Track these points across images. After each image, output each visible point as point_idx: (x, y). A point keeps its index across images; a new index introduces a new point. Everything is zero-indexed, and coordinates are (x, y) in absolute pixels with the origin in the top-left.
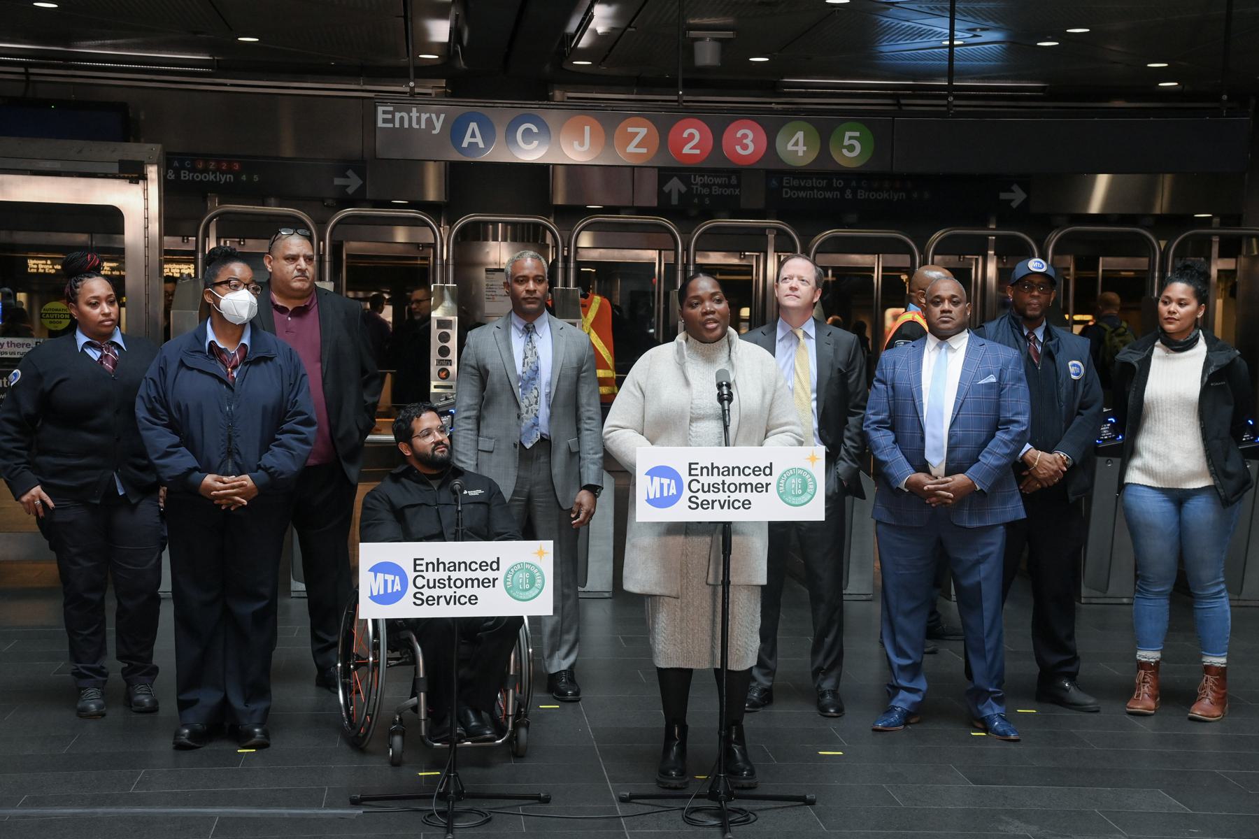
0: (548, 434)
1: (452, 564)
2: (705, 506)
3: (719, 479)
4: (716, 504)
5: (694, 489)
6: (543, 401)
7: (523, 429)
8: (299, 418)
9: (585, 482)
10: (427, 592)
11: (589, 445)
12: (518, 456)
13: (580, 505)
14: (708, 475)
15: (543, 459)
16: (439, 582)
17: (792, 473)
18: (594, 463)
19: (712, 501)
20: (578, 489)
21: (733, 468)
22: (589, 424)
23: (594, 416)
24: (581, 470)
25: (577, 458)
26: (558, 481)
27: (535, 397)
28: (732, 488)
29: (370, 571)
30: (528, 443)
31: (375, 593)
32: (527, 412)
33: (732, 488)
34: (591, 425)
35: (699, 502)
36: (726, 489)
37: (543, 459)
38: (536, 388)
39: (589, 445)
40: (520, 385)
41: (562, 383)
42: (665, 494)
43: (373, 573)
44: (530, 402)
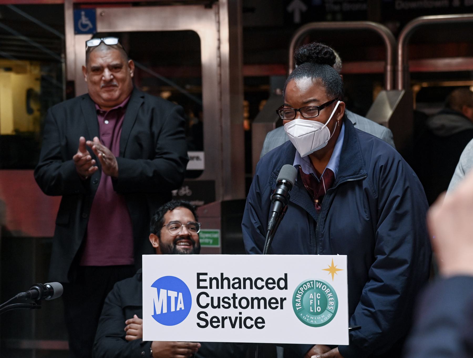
3: (229, 293)
4: (227, 322)
14: (218, 287)
17: (309, 286)
21: (245, 280)
28: (244, 303)
33: (244, 303)
35: (208, 319)
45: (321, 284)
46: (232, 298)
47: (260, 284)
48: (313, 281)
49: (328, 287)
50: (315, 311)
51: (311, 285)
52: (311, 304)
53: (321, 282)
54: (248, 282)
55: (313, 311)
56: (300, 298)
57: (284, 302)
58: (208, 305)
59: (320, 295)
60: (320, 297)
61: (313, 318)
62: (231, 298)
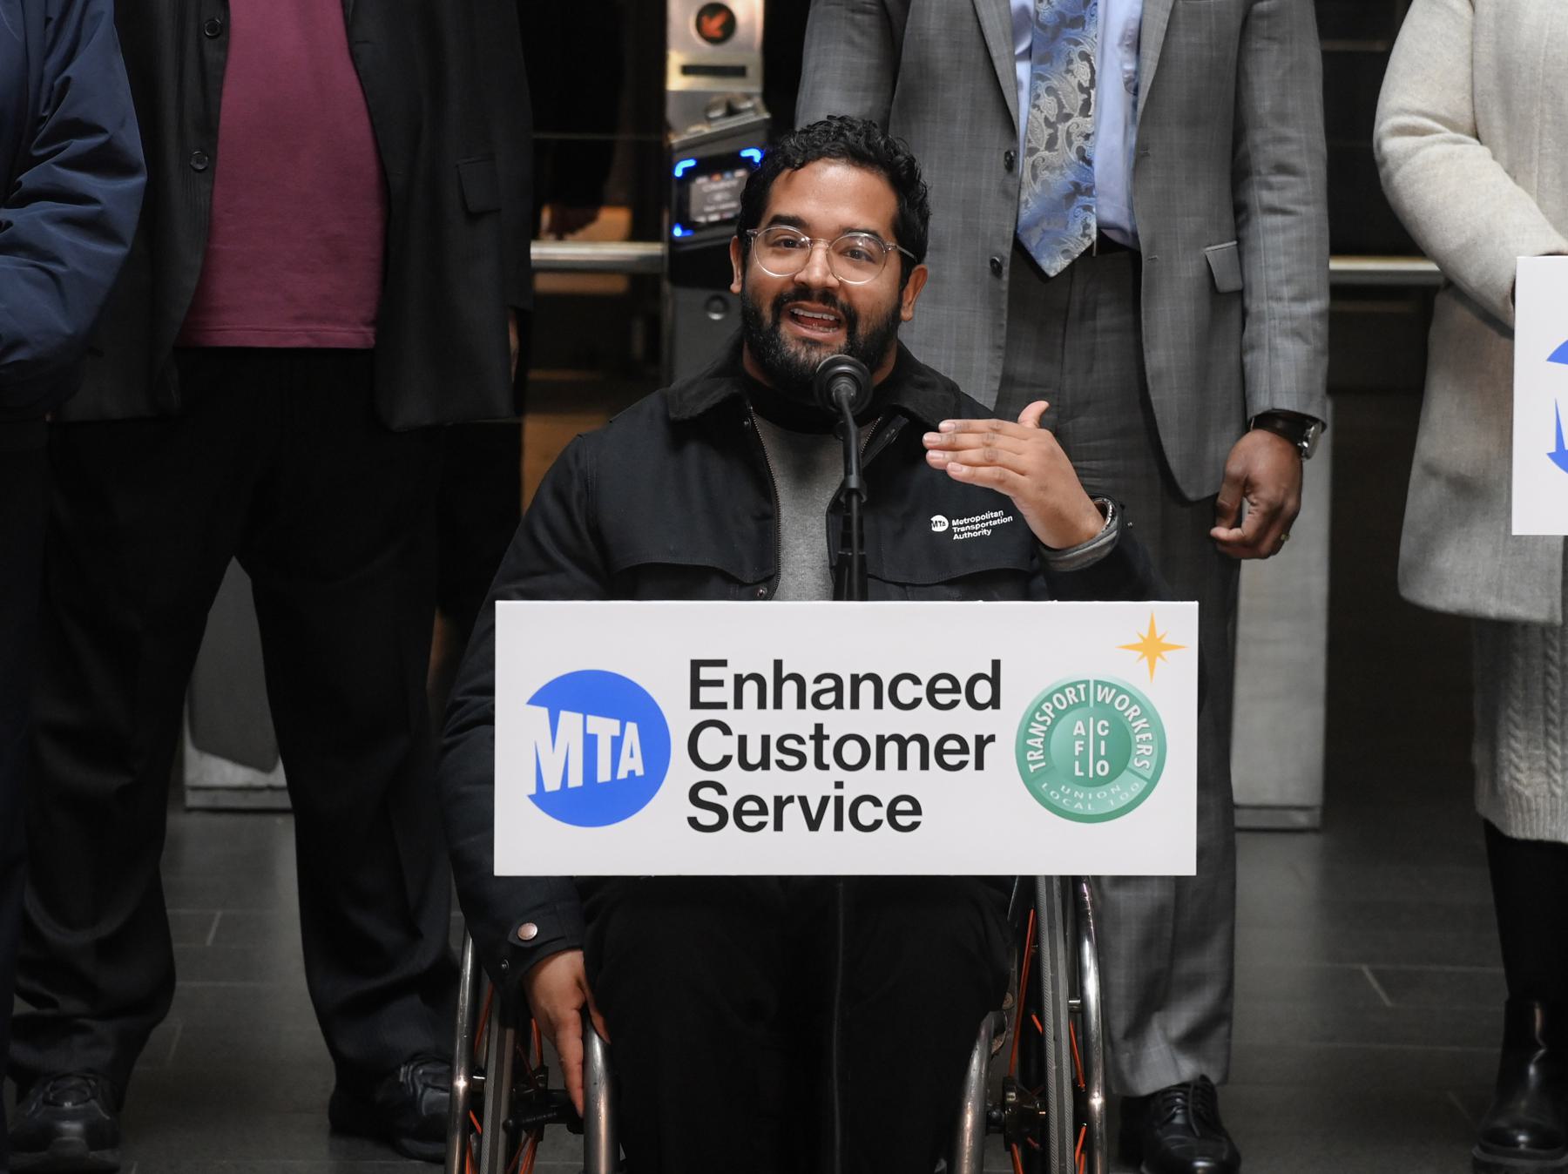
0: (1127, 226)
1: (829, 683)
2: (750, 821)
3: (802, 722)
4: (793, 813)
5: (710, 757)
6: (1112, 103)
7: (1025, 214)
8: (79, 145)
9: (1262, 403)
10: (738, 783)
11: (1277, 267)
12: (1005, 306)
13: (1246, 485)
14: (762, 704)
15: (1106, 317)
16: (781, 747)
17: (1072, 697)
18: (1297, 334)
19: (778, 800)
20: (1234, 427)
21: (856, 680)
22: (1282, 188)
23: (1296, 161)
24: (1248, 359)
25: (1235, 314)
26: (1168, 398)
27: (1081, 88)
28: (852, 752)
29: (536, 700)
30: (1052, 256)
31: (552, 784)
32: (1051, 144)
33: (852, 752)
34: (1289, 194)
35: (728, 803)
36: (828, 757)
37: (1106, 317)
38: (1085, 57)
39: (1277, 267)
40: (1022, 47)
41: (1181, 39)
42: (604, 775)
43: (543, 713)
44: (1061, 106)
45: (1114, 691)
46: (811, 737)
47: (906, 692)
48: (1087, 682)
49: (1134, 700)
50: (1091, 775)
51: (1078, 695)
52: (1077, 753)
53: (1111, 686)
54: (867, 689)
55: (1082, 774)
56: (1043, 735)
57: (989, 748)
58: (726, 760)
59: (1107, 724)
60: (1107, 732)
61: (1082, 796)
62: (806, 738)
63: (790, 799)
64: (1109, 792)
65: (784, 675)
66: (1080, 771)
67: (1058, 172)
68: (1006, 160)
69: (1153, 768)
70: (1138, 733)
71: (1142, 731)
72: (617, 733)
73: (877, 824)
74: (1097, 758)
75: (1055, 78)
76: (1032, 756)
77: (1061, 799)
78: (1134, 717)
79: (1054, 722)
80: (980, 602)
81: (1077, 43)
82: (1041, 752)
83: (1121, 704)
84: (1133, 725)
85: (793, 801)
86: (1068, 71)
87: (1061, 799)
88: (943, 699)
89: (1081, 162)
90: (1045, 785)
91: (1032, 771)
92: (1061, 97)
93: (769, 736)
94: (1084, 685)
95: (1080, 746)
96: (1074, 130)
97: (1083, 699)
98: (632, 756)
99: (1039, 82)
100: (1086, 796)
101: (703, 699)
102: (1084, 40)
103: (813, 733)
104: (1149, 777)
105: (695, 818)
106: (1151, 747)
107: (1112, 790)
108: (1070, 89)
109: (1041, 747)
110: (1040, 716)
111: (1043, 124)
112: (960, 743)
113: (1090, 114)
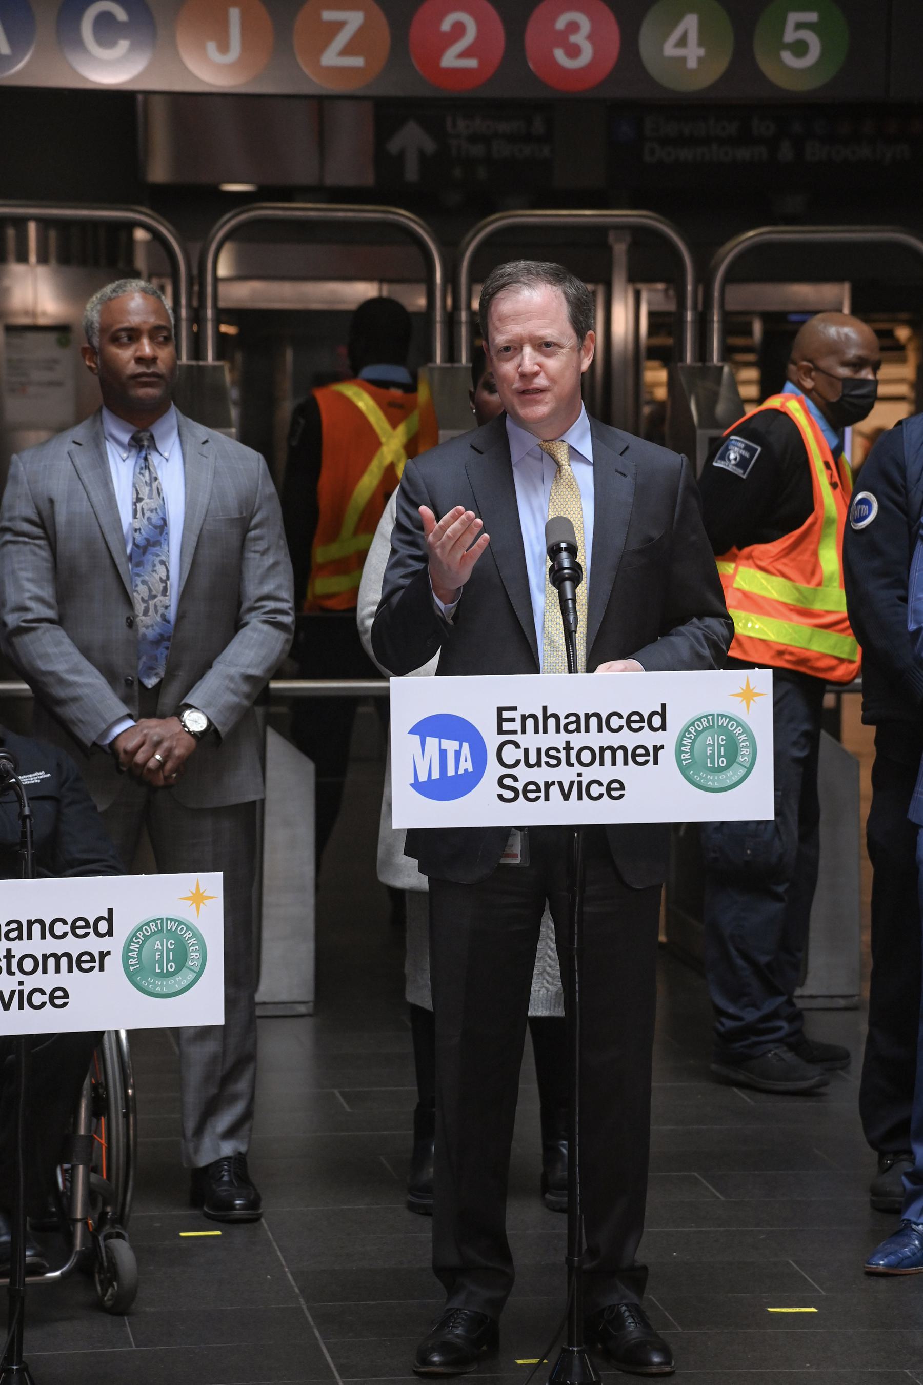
2: (531, 796)
3: (560, 740)
4: (555, 791)
14: (536, 731)
21: (587, 717)
28: (586, 757)
30: (149, 677)
32: (146, 612)
33: (586, 757)
35: (519, 786)
36: (573, 760)
38: (163, 563)
42: (451, 772)
44: (150, 590)
45: (728, 719)
46: (564, 749)
47: (615, 722)
48: (713, 715)
49: (739, 724)
50: (716, 766)
51: (708, 722)
52: (708, 754)
53: (726, 717)
54: (593, 721)
55: (711, 766)
56: (690, 745)
57: (661, 753)
59: (724, 738)
60: (724, 742)
61: (711, 778)
62: (561, 749)
63: (553, 783)
64: (175, 980)
65: (548, 715)
66: (710, 764)
67: (150, 628)
68: (127, 621)
69: (750, 761)
70: (742, 742)
71: (744, 741)
72: (458, 749)
73: (43, 1004)
74: (168, 961)
75: (146, 575)
76: (684, 756)
77: (148, 986)
78: (739, 733)
79: (144, 942)
80: (101, 877)
81: (158, 555)
82: (689, 754)
83: (181, 931)
84: (739, 738)
85: (555, 785)
86: (154, 571)
87: (148, 986)
88: (80, 932)
89: (164, 622)
90: (692, 772)
91: (684, 764)
92: (150, 585)
93: (541, 749)
94: (711, 717)
95: (710, 750)
96: (159, 604)
97: (711, 724)
98: (466, 761)
99: (137, 577)
100: (714, 777)
101: (504, 729)
102: (162, 553)
103: (565, 746)
104: (748, 766)
105: (501, 795)
106: (198, 954)
107: (728, 774)
108: (155, 581)
109: (689, 751)
110: (688, 734)
111: (141, 601)
112: (645, 750)
113: (167, 594)
